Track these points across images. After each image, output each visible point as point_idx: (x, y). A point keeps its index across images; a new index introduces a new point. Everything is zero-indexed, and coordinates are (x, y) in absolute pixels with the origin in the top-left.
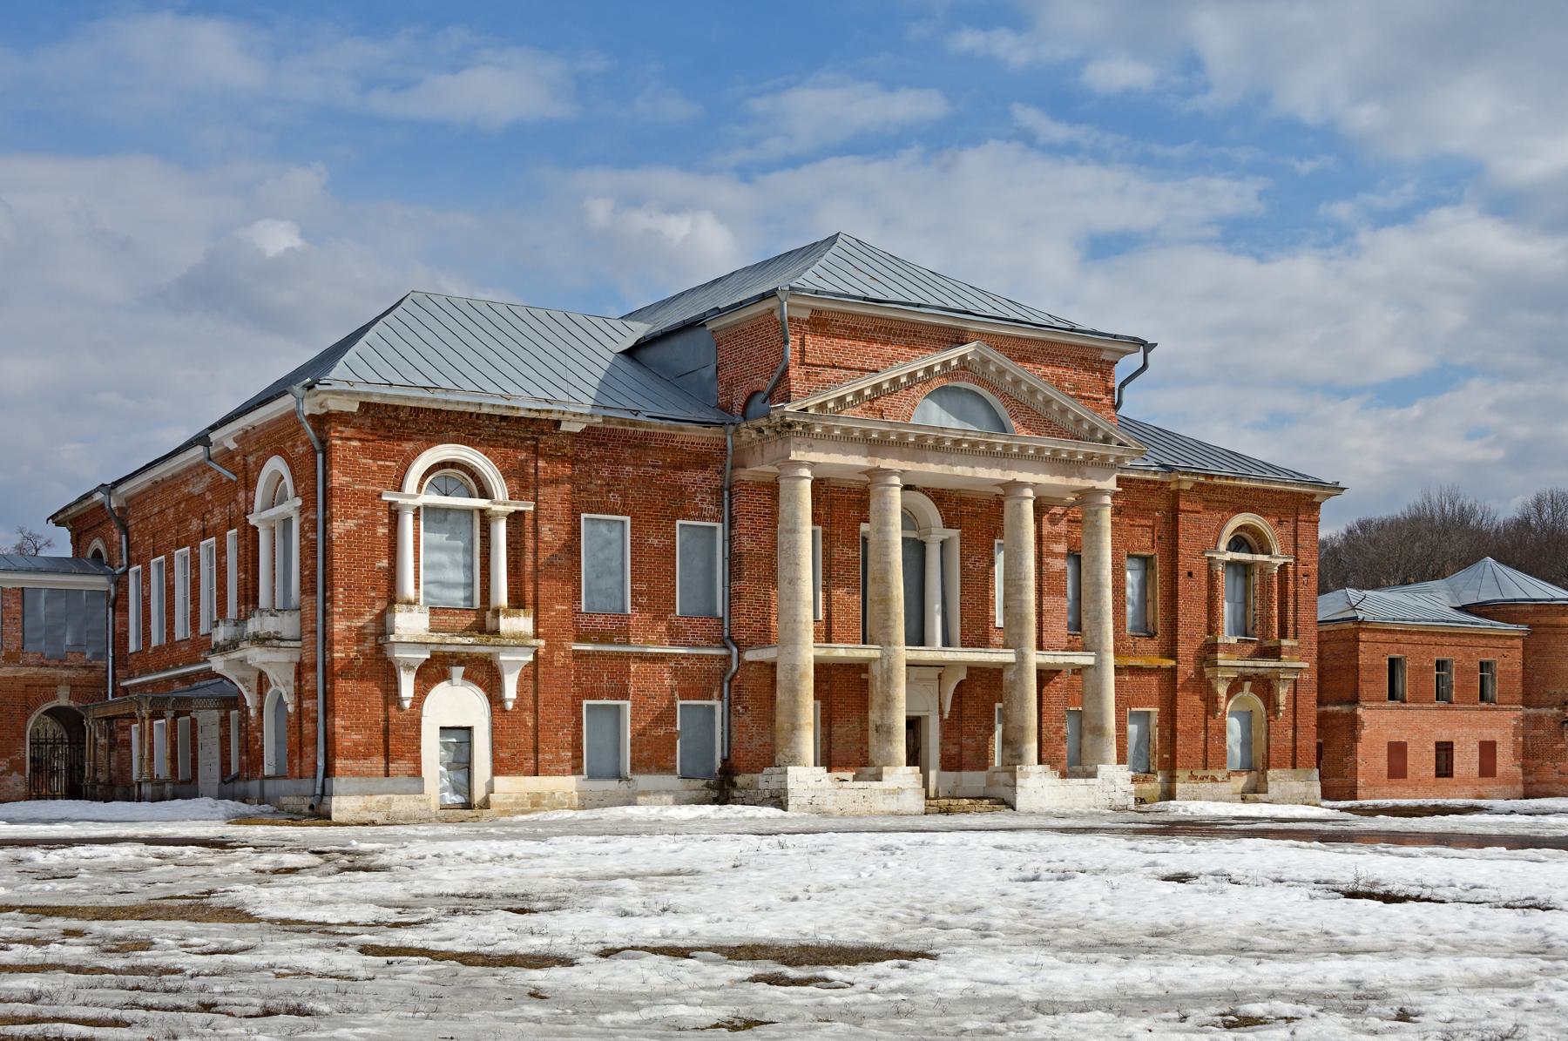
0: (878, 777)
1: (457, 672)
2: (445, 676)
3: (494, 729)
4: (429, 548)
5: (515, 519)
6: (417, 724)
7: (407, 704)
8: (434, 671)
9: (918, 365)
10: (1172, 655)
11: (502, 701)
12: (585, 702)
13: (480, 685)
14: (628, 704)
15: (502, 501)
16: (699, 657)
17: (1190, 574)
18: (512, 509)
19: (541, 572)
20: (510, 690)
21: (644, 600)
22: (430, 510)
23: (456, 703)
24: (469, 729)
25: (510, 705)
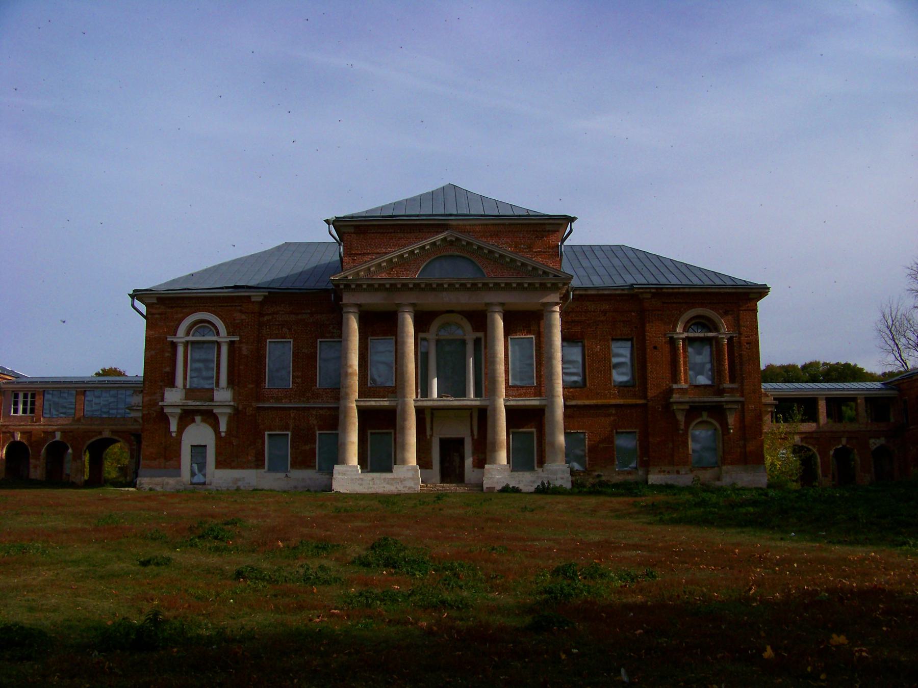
0: (390, 470)
1: (198, 419)
2: (193, 421)
3: (217, 445)
4: (193, 361)
5: (232, 343)
6: (179, 442)
7: (174, 435)
8: (187, 416)
9: (415, 247)
10: (645, 397)
11: (220, 433)
12: (267, 433)
13: (210, 425)
14: (289, 433)
15: (224, 336)
16: (329, 408)
17: (655, 348)
18: (228, 340)
19: (246, 370)
20: (223, 427)
21: (299, 381)
22: (193, 343)
23: (199, 434)
24: (205, 446)
25: (223, 434)
